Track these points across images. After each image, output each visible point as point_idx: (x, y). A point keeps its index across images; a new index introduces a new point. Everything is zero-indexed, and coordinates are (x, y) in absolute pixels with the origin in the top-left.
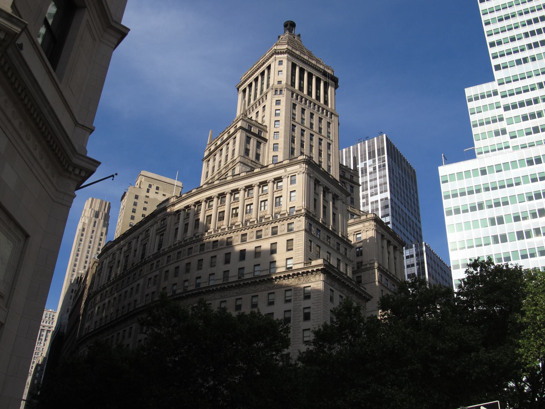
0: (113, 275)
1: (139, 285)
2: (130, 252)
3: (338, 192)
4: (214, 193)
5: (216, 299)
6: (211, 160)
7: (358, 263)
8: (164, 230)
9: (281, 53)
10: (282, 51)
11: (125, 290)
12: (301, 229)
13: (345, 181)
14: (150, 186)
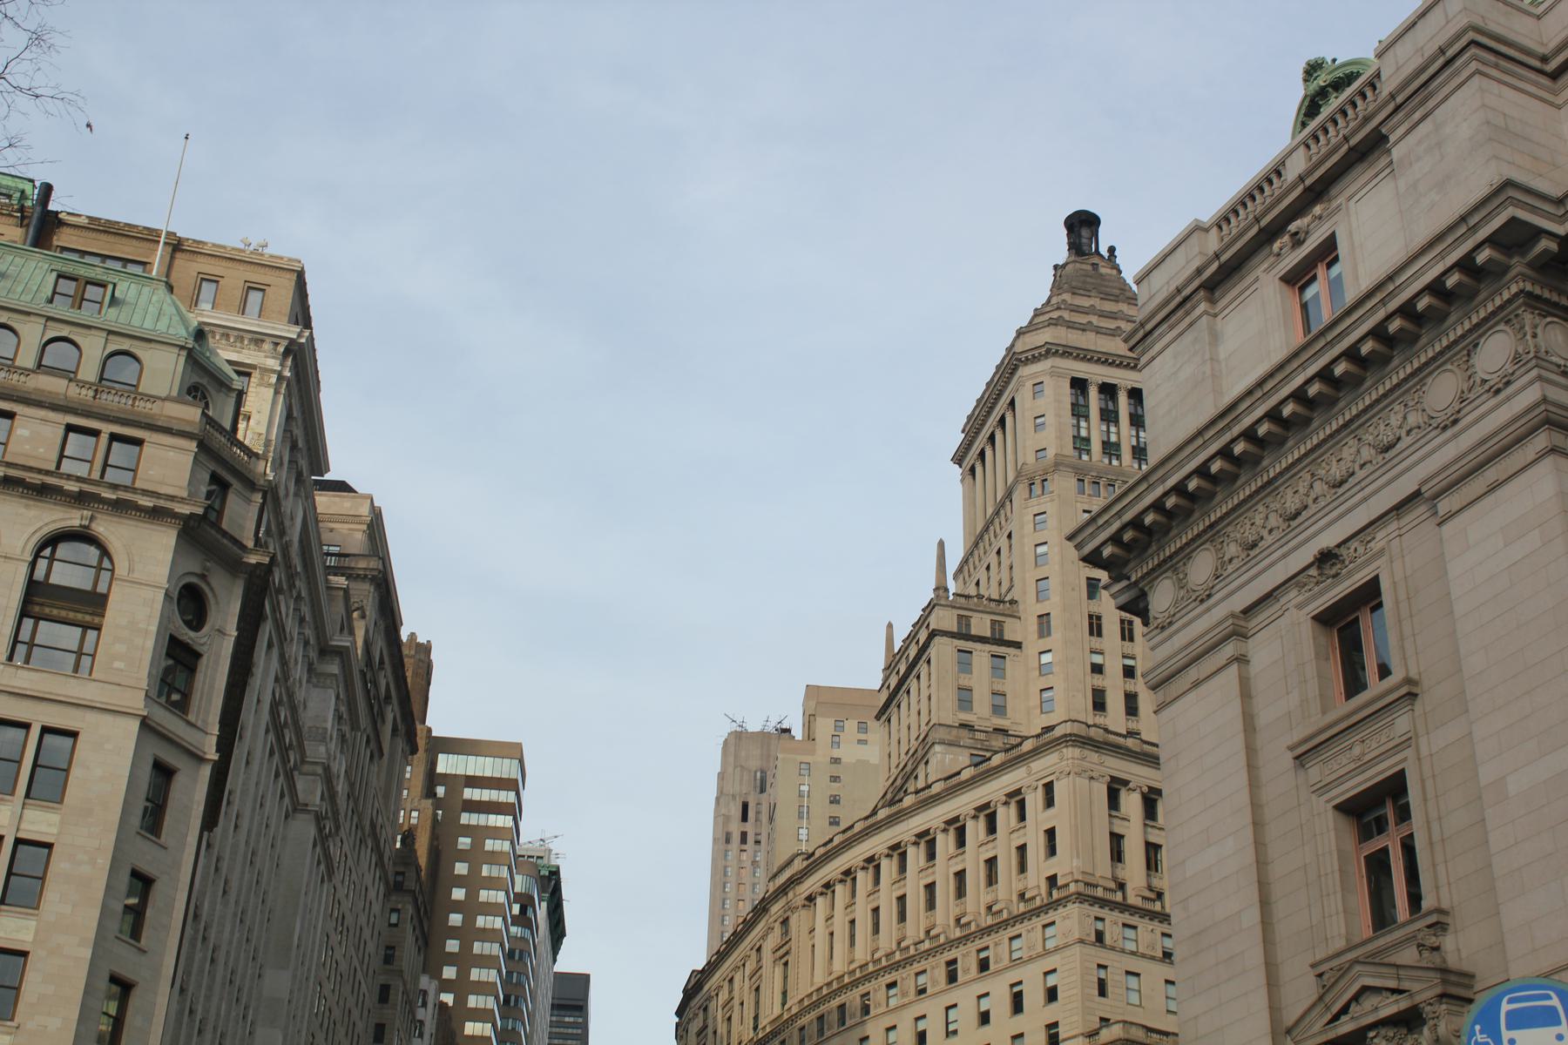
4: (877, 844)
8: (787, 953)
9: (1035, 359)
10: (1036, 353)
12: (1070, 940)
14: (839, 725)
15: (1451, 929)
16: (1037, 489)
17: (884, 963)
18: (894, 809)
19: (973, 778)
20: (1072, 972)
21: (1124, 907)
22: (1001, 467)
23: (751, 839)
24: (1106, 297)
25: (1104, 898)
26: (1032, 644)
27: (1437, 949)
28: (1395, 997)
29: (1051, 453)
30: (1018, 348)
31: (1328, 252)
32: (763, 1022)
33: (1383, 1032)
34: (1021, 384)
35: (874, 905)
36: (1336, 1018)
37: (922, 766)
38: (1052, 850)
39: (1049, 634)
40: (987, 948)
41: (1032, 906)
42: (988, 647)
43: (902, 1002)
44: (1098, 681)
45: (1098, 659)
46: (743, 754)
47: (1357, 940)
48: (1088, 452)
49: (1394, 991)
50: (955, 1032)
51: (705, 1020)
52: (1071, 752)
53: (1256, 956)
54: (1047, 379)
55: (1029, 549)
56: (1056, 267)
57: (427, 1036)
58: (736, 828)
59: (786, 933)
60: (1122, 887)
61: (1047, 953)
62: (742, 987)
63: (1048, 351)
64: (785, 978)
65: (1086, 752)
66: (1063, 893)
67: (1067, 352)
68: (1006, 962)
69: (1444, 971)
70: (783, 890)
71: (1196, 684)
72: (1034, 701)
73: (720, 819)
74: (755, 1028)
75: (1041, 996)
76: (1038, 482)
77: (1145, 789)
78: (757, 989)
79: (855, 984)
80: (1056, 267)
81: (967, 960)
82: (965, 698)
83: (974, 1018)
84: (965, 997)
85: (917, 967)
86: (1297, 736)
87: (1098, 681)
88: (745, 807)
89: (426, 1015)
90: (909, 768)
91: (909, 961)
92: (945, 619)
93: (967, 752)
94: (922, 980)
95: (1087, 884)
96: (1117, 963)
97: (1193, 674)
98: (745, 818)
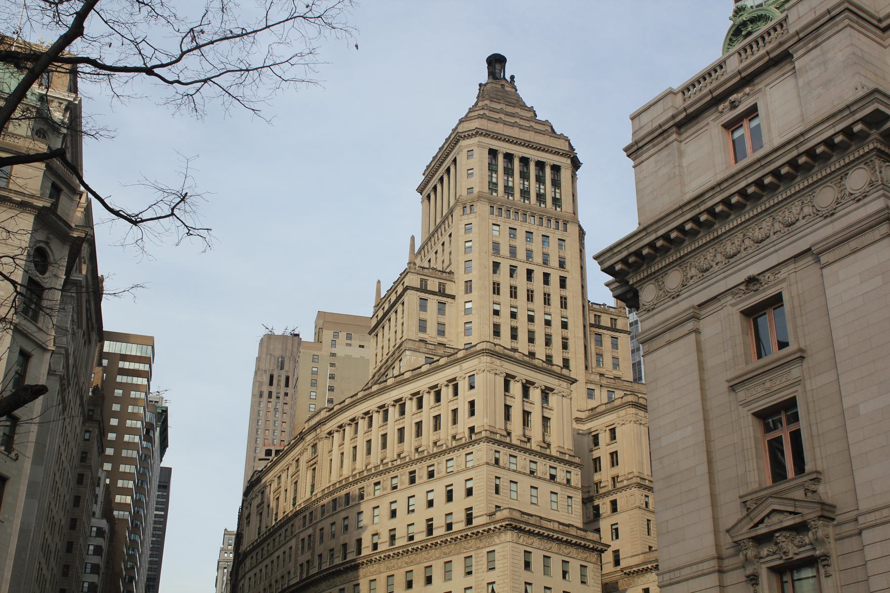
0: (263, 530)
1: (291, 548)
2: (280, 493)
3: (551, 382)
4: (371, 405)
5: (381, 572)
6: (380, 335)
7: (613, 479)
9: (470, 136)
10: (470, 133)
11: (276, 554)
12: (481, 462)
13: (601, 331)
14: (336, 335)
15: (823, 481)
16: (468, 210)
17: (373, 471)
18: (382, 385)
19: (428, 370)
20: (481, 480)
21: (510, 446)
22: (446, 197)
23: (274, 395)
24: (509, 104)
25: (499, 440)
26: (461, 296)
27: (814, 492)
28: (792, 516)
29: (476, 191)
30: (460, 130)
31: (752, 112)
32: (299, 501)
33: (784, 533)
34: (460, 150)
35: (368, 439)
36: (756, 525)
37: (398, 362)
38: (472, 413)
39: (471, 292)
40: (433, 465)
41: (460, 443)
42: (436, 297)
43: (382, 493)
44: (497, 319)
45: (497, 307)
46: (272, 347)
47: (764, 486)
48: (496, 191)
49: (791, 513)
50: (413, 511)
51: (262, 499)
52: (485, 359)
53: (705, 490)
54: (475, 148)
55: (461, 244)
56: (480, 85)
57: (99, 503)
58: (266, 389)
59: (315, 452)
60: (509, 434)
61: (467, 469)
62: (286, 482)
63: (477, 133)
64: (314, 477)
66: (478, 437)
67: (487, 134)
68: (444, 473)
69: (823, 504)
70: (314, 428)
71: (669, 343)
72: (461, 328)
73: (257, 384)
74: (294, 504)
75: (463, 493)
76: (468, 206)
77: (524, 381)
78: (296, 483)
79: (356, 482)
80: (480, 85)
81: (421, 471)
82: (423, 326)
83: (424, 504)
84: (420, 492)
85: (392, 474)
86: (730, 375)
87: (497, 319)
88: (272, 377)
89: (100, 491)
90: (389, 363)
91: (388, 471)
93: (424, 356)
94: (395, 481)
95: (491, 432)
96: (507, 477)
97: (667, 337)
98: (271, 384)
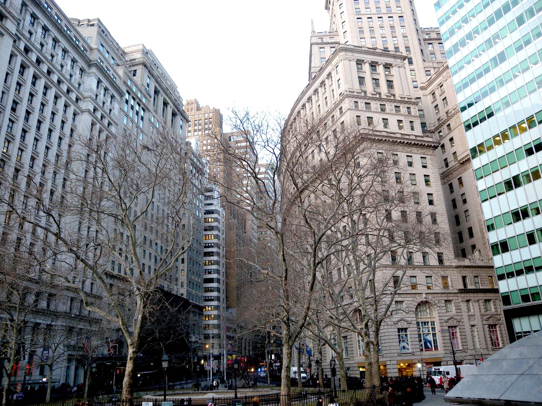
52: (341, 54)
65: (347, 53)
92: (315, 40)
